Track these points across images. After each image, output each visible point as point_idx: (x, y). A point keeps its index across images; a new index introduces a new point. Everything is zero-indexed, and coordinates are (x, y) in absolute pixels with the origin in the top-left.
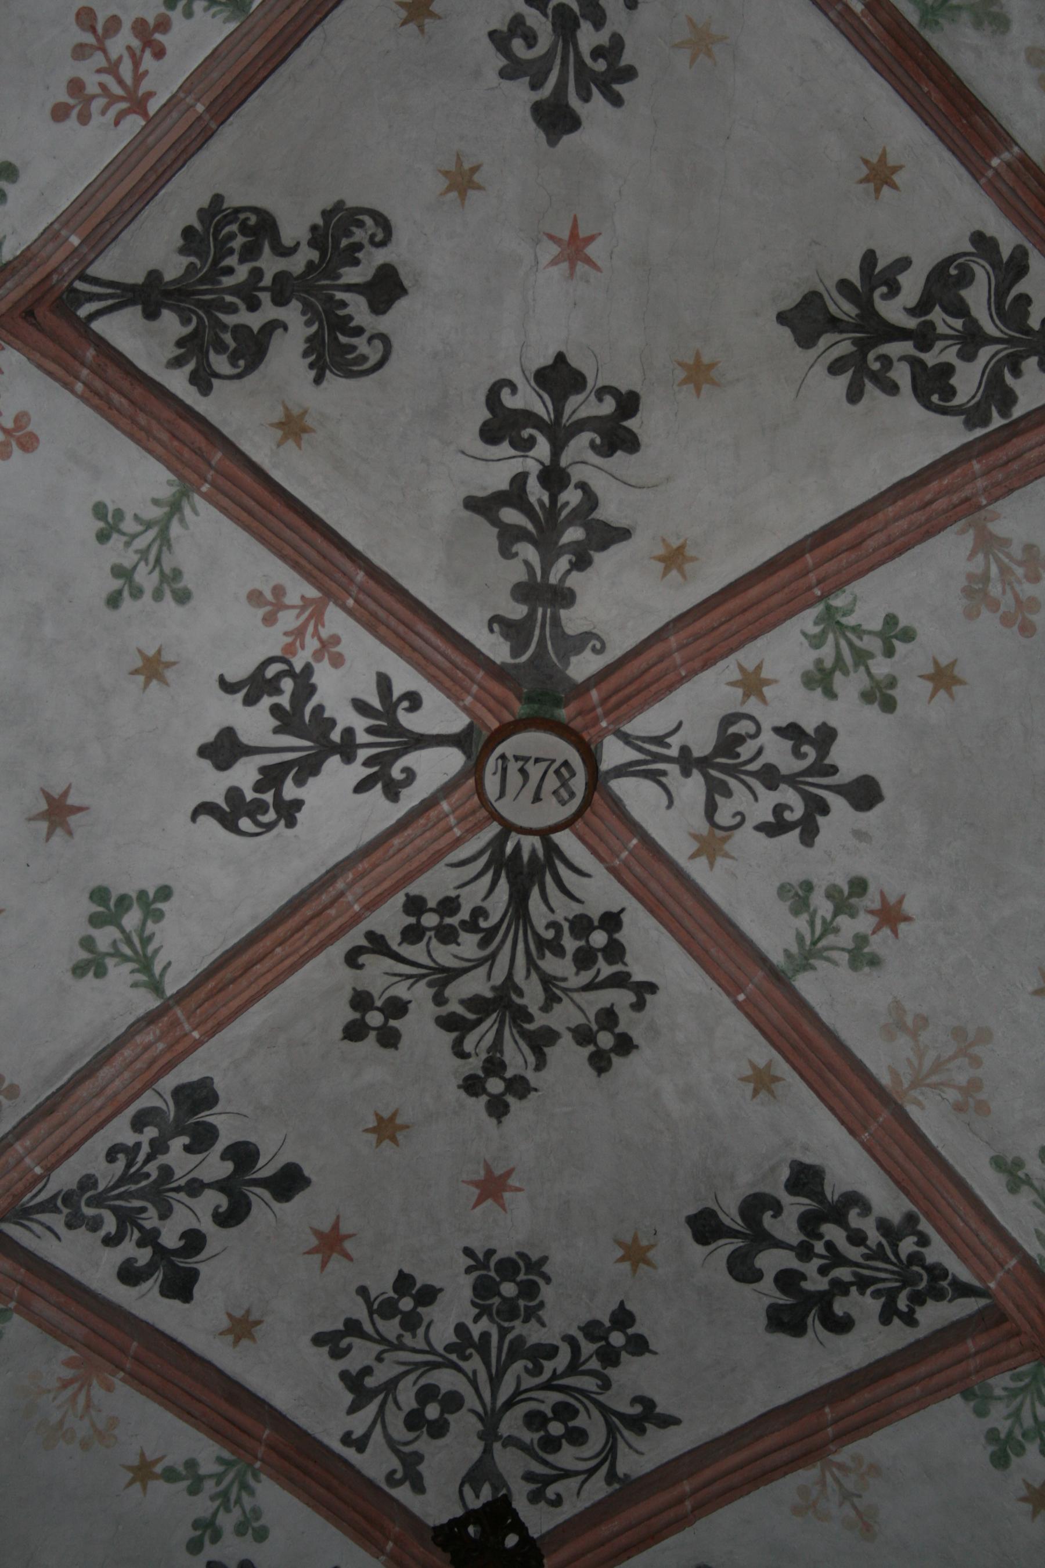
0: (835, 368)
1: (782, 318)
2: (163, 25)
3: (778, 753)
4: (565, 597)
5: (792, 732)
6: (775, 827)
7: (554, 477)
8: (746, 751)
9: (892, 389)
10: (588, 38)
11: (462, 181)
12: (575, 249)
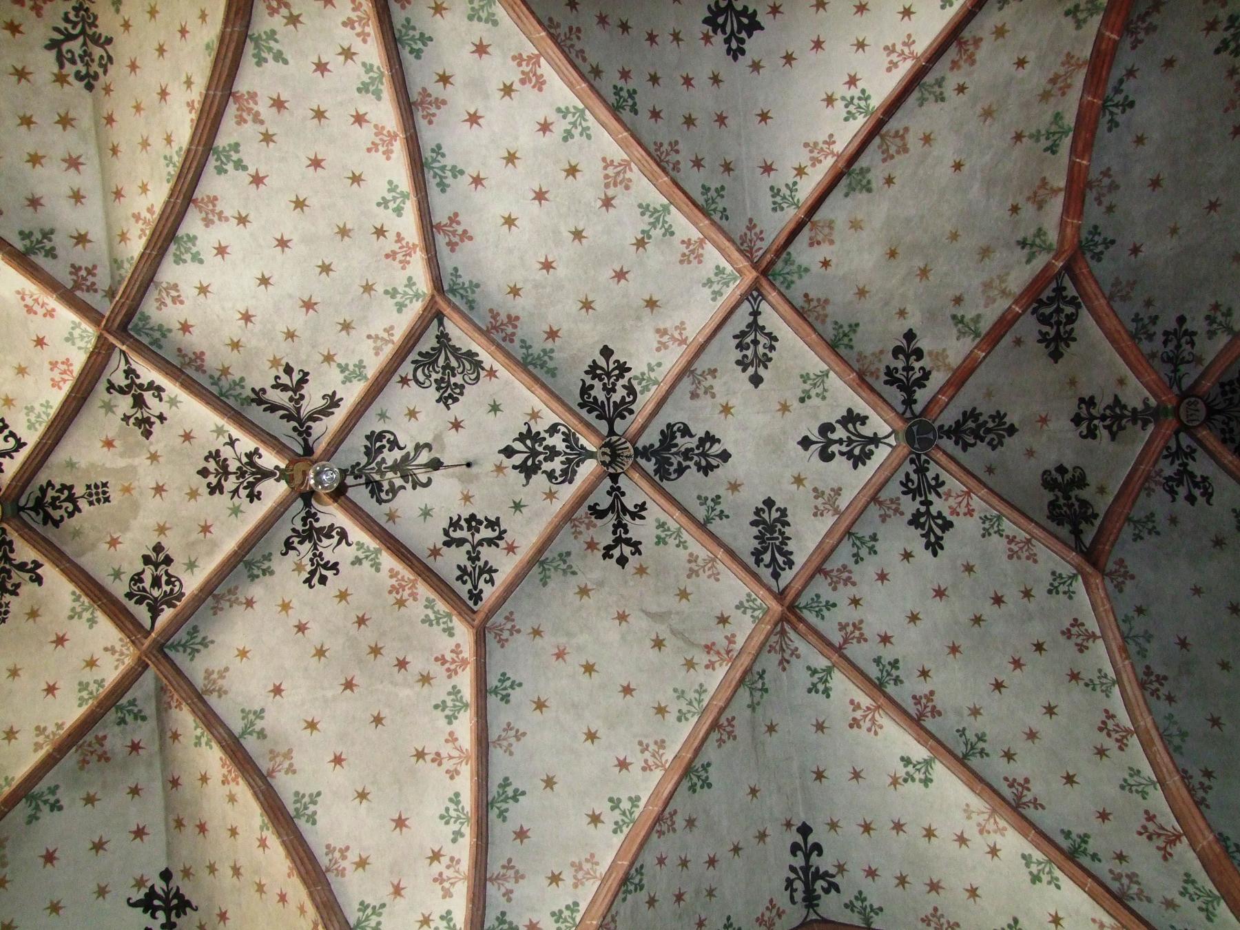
0: (1068, 346)
1: (1056, 362)
2: (1007, 537)
3: (1171, 346)
4: (1134, 409)
5: (1165, 343)
6: (1192, 344)
7: (1103, 418)
8: (1171, 354)
9: (1072, 330)
10: (990, 425)
11: (1030, 453)
12: (1044, 420)
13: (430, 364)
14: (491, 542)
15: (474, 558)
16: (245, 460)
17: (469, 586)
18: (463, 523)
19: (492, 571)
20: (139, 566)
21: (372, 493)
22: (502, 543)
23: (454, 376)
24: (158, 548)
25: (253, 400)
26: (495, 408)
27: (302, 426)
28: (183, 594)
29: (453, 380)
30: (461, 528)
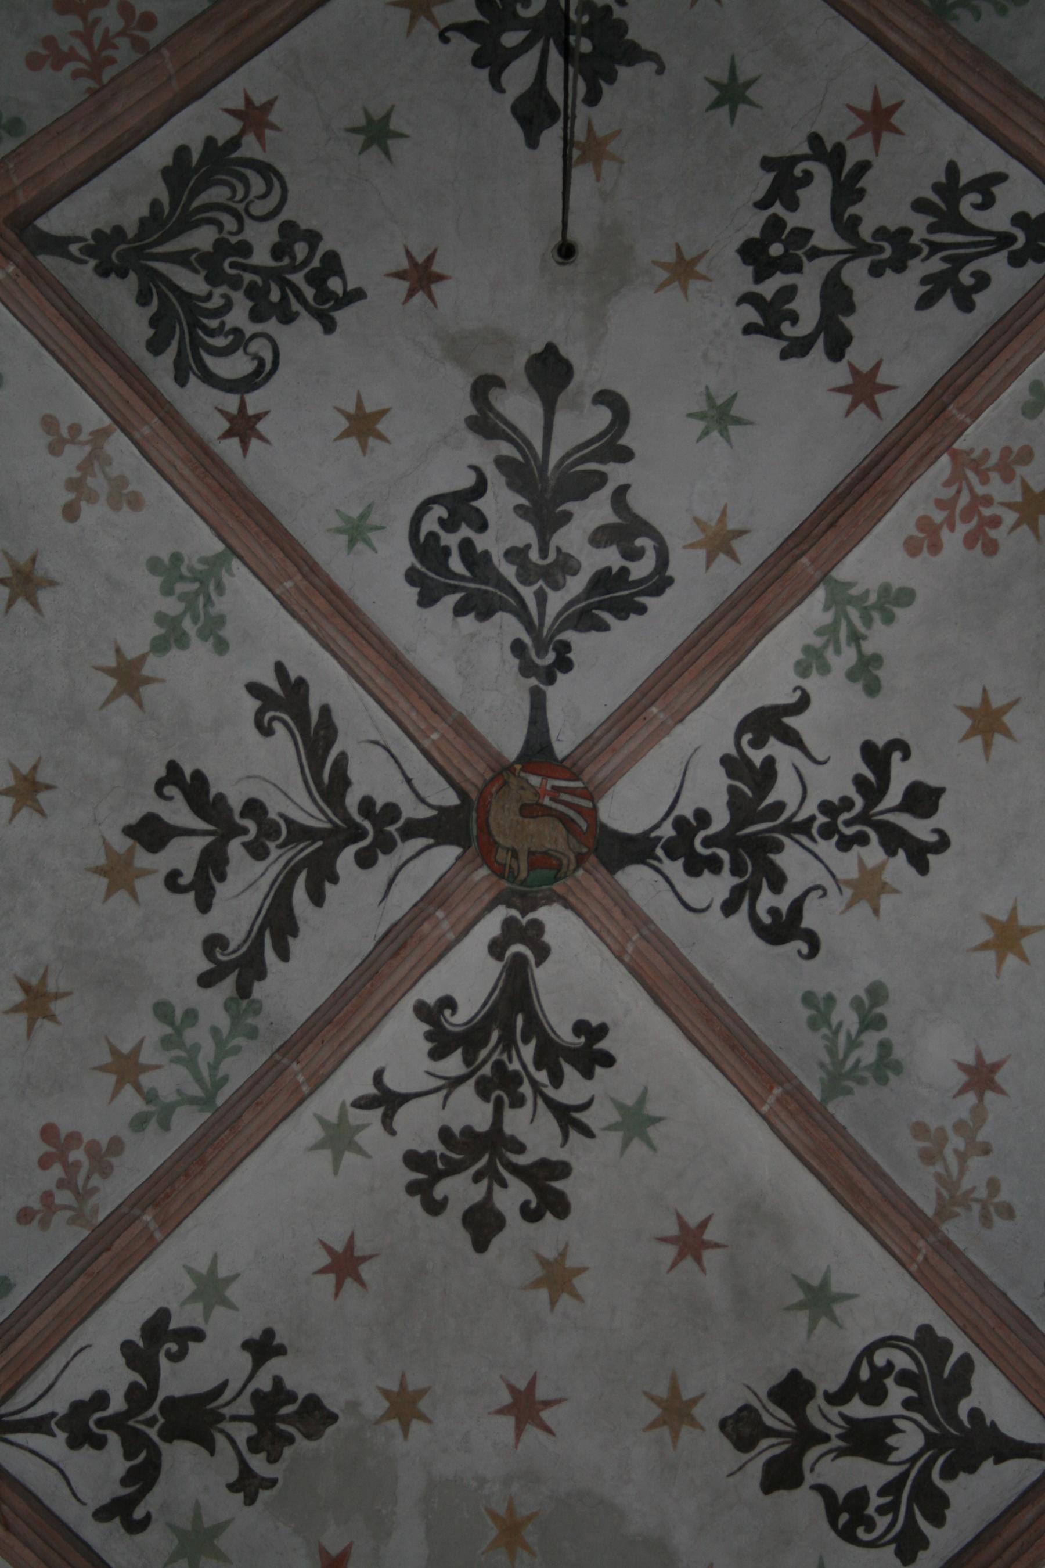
13: (194, 325)
14: (848, 189)
15: (896, 250)
16: (454, 1064)
17: (996, 264)
18: (768, 289)
19: (951, 186)
20: (802, 1505)
21: (627, 608)
22: (857, 152)
23: (245, 249)
24: (742, 1427)
25: (244, 991)
26: (377, 133)
27: (359, 834)
28: (925, 1331)
29: (262, 257)
30: (789, 293)
